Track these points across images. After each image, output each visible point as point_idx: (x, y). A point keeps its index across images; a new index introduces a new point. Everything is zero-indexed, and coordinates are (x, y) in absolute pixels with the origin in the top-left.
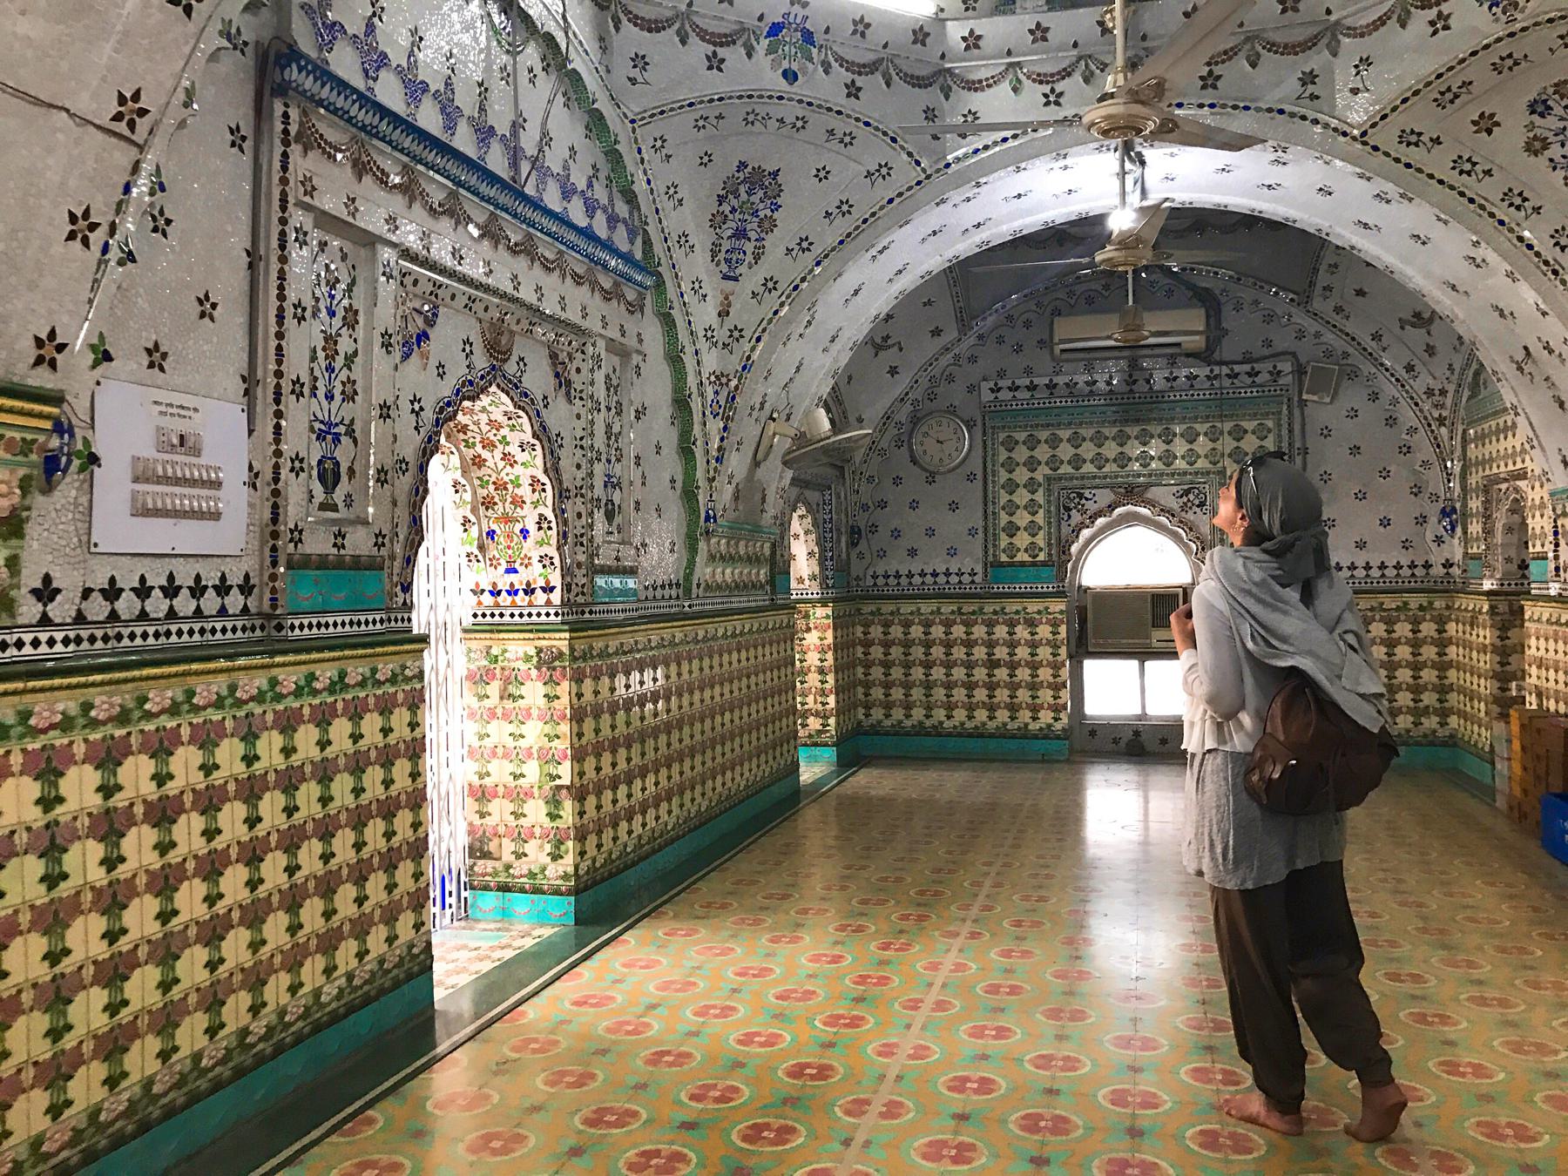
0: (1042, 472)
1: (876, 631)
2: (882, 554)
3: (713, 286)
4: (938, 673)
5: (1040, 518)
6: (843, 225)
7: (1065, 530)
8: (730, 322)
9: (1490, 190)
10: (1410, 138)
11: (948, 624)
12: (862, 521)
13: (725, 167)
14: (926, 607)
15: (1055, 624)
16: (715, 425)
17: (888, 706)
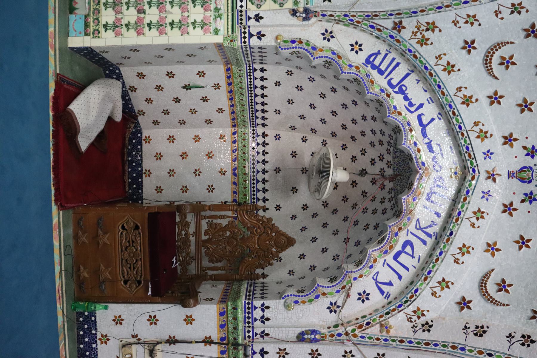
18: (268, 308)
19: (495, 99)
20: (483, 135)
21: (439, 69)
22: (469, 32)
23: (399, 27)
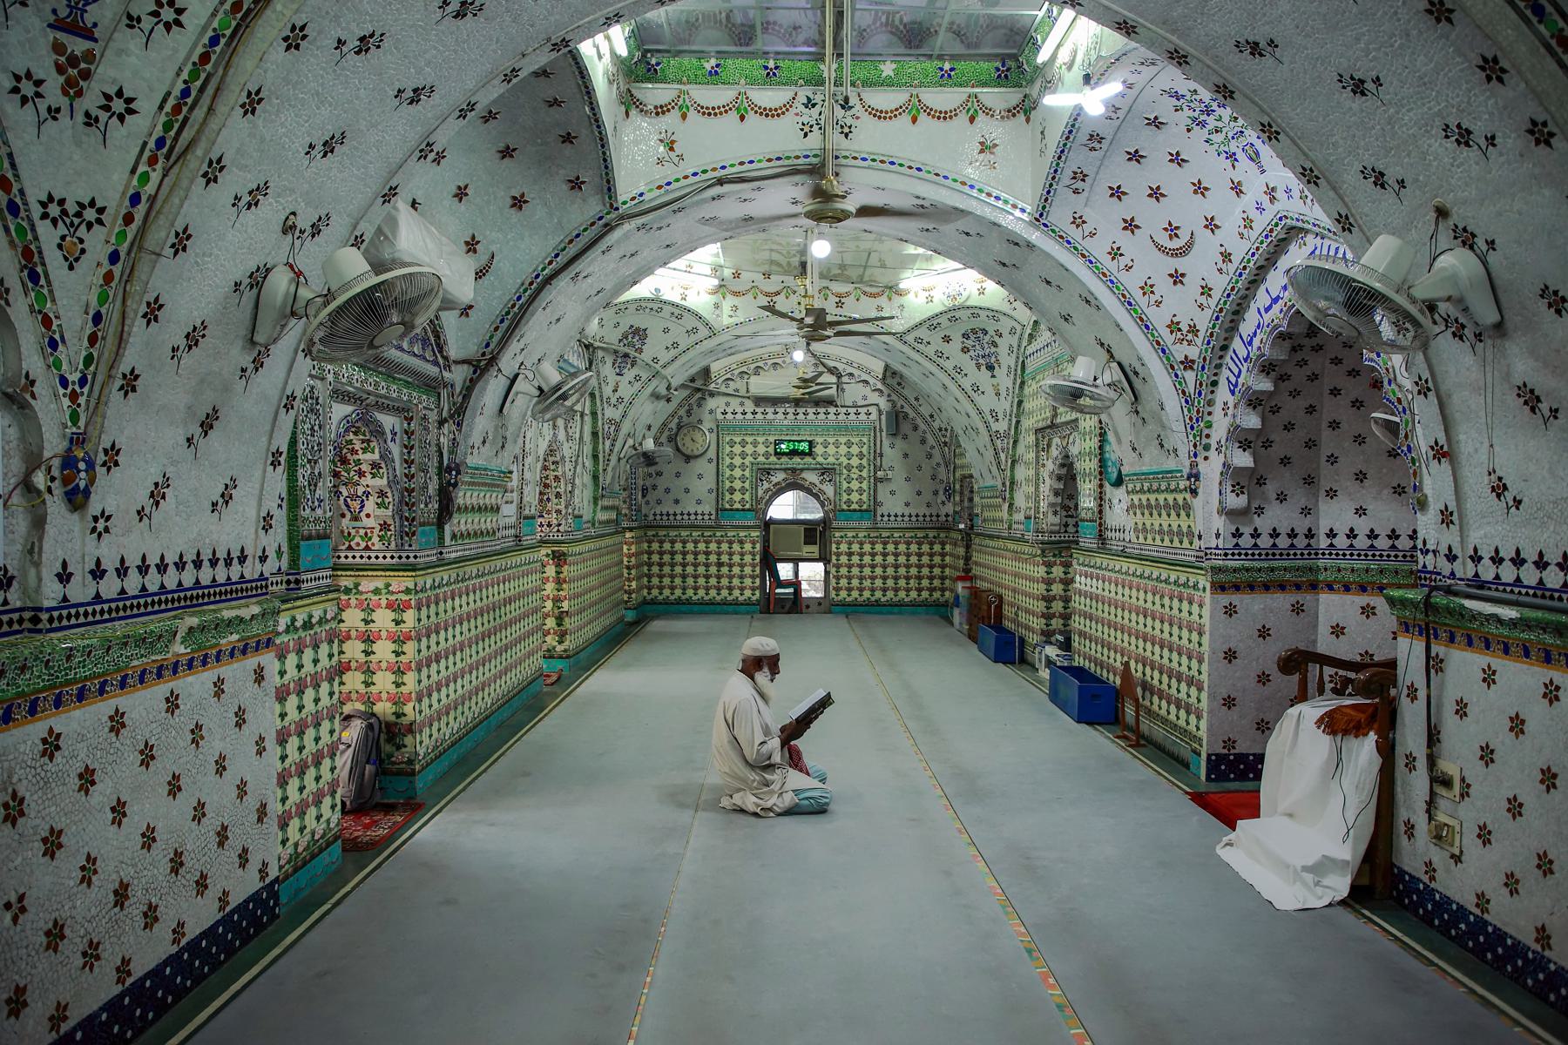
0: (749, 459)
1: (655, 546)
2: (659, 502)
3: (612, 378)
4: (690, 569)
5: (747, 485)
6: (673, 353)
7: (760, 492)
8: (617, 395)
9: (949, 365)
10: (919, 340)
11: (696, 542)
12: (648, 483)
13: (624, 328)
14: (684, 533)
15: (754, 543)
16: (608, 443)
17: (661, 588)
18: (1425, 543)
19: (1211, 225)
20: (1248, 223)
21: (1212, 303)
22: (1163, 286)
23: (1188, 364)
